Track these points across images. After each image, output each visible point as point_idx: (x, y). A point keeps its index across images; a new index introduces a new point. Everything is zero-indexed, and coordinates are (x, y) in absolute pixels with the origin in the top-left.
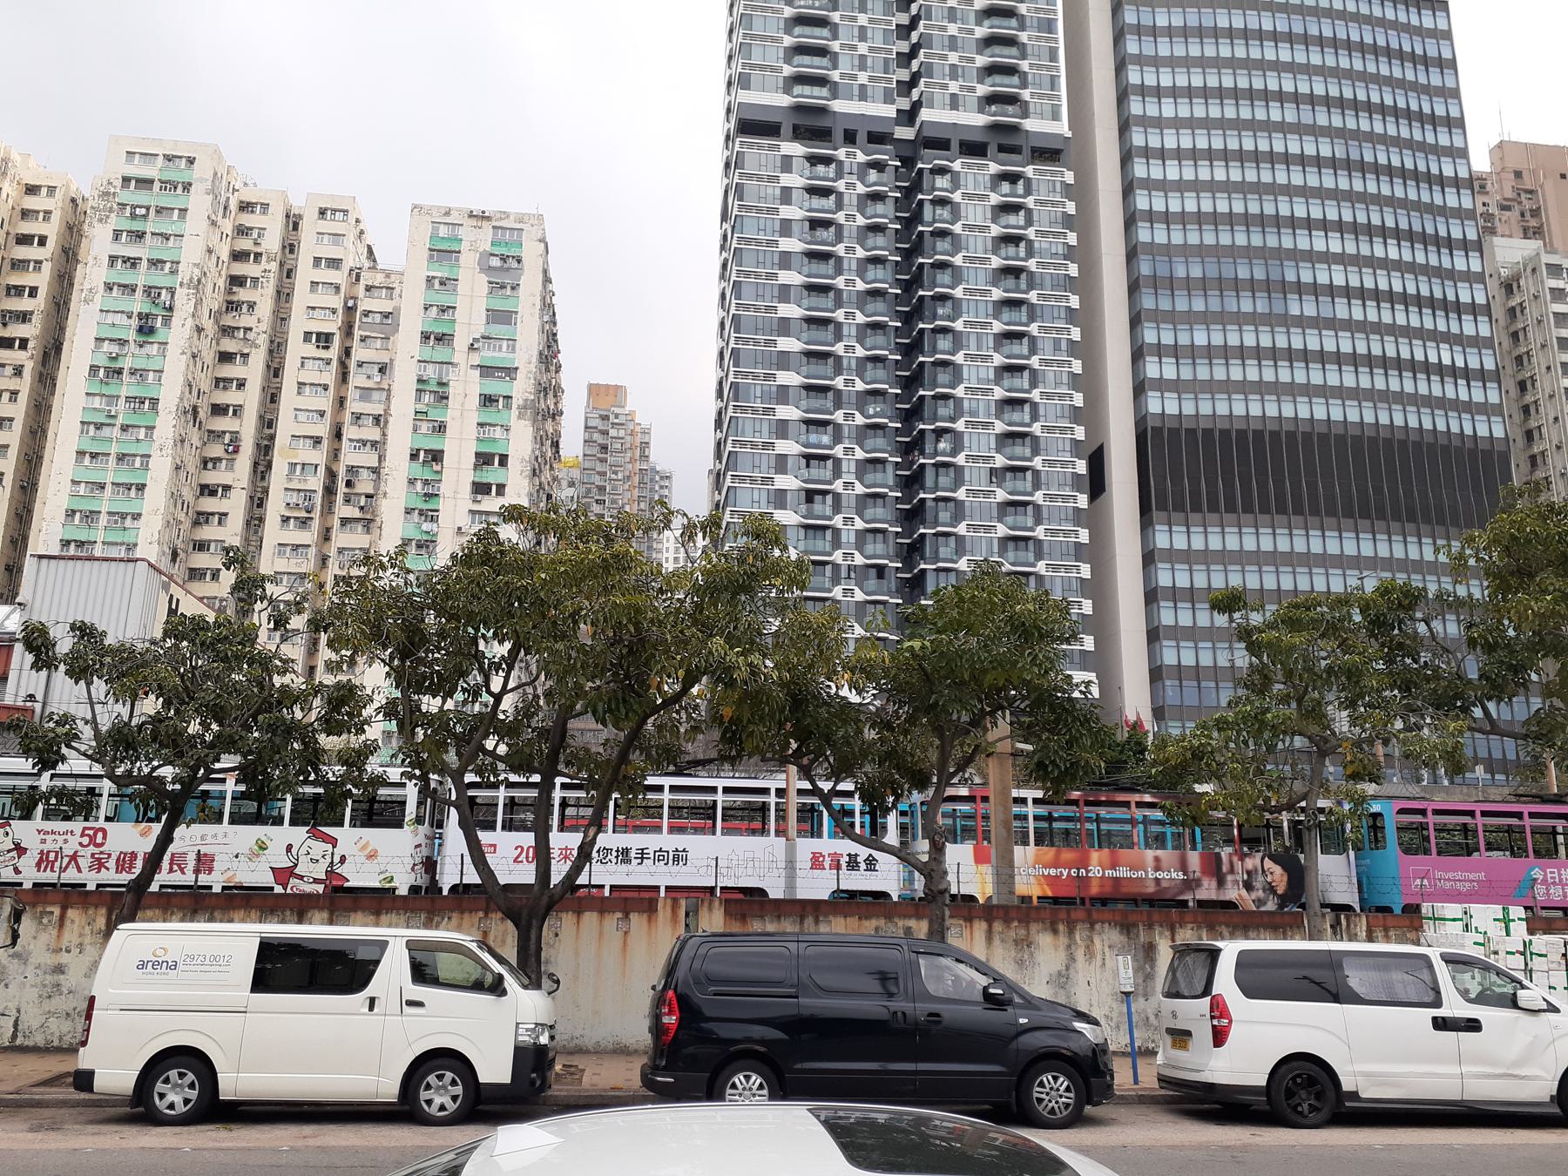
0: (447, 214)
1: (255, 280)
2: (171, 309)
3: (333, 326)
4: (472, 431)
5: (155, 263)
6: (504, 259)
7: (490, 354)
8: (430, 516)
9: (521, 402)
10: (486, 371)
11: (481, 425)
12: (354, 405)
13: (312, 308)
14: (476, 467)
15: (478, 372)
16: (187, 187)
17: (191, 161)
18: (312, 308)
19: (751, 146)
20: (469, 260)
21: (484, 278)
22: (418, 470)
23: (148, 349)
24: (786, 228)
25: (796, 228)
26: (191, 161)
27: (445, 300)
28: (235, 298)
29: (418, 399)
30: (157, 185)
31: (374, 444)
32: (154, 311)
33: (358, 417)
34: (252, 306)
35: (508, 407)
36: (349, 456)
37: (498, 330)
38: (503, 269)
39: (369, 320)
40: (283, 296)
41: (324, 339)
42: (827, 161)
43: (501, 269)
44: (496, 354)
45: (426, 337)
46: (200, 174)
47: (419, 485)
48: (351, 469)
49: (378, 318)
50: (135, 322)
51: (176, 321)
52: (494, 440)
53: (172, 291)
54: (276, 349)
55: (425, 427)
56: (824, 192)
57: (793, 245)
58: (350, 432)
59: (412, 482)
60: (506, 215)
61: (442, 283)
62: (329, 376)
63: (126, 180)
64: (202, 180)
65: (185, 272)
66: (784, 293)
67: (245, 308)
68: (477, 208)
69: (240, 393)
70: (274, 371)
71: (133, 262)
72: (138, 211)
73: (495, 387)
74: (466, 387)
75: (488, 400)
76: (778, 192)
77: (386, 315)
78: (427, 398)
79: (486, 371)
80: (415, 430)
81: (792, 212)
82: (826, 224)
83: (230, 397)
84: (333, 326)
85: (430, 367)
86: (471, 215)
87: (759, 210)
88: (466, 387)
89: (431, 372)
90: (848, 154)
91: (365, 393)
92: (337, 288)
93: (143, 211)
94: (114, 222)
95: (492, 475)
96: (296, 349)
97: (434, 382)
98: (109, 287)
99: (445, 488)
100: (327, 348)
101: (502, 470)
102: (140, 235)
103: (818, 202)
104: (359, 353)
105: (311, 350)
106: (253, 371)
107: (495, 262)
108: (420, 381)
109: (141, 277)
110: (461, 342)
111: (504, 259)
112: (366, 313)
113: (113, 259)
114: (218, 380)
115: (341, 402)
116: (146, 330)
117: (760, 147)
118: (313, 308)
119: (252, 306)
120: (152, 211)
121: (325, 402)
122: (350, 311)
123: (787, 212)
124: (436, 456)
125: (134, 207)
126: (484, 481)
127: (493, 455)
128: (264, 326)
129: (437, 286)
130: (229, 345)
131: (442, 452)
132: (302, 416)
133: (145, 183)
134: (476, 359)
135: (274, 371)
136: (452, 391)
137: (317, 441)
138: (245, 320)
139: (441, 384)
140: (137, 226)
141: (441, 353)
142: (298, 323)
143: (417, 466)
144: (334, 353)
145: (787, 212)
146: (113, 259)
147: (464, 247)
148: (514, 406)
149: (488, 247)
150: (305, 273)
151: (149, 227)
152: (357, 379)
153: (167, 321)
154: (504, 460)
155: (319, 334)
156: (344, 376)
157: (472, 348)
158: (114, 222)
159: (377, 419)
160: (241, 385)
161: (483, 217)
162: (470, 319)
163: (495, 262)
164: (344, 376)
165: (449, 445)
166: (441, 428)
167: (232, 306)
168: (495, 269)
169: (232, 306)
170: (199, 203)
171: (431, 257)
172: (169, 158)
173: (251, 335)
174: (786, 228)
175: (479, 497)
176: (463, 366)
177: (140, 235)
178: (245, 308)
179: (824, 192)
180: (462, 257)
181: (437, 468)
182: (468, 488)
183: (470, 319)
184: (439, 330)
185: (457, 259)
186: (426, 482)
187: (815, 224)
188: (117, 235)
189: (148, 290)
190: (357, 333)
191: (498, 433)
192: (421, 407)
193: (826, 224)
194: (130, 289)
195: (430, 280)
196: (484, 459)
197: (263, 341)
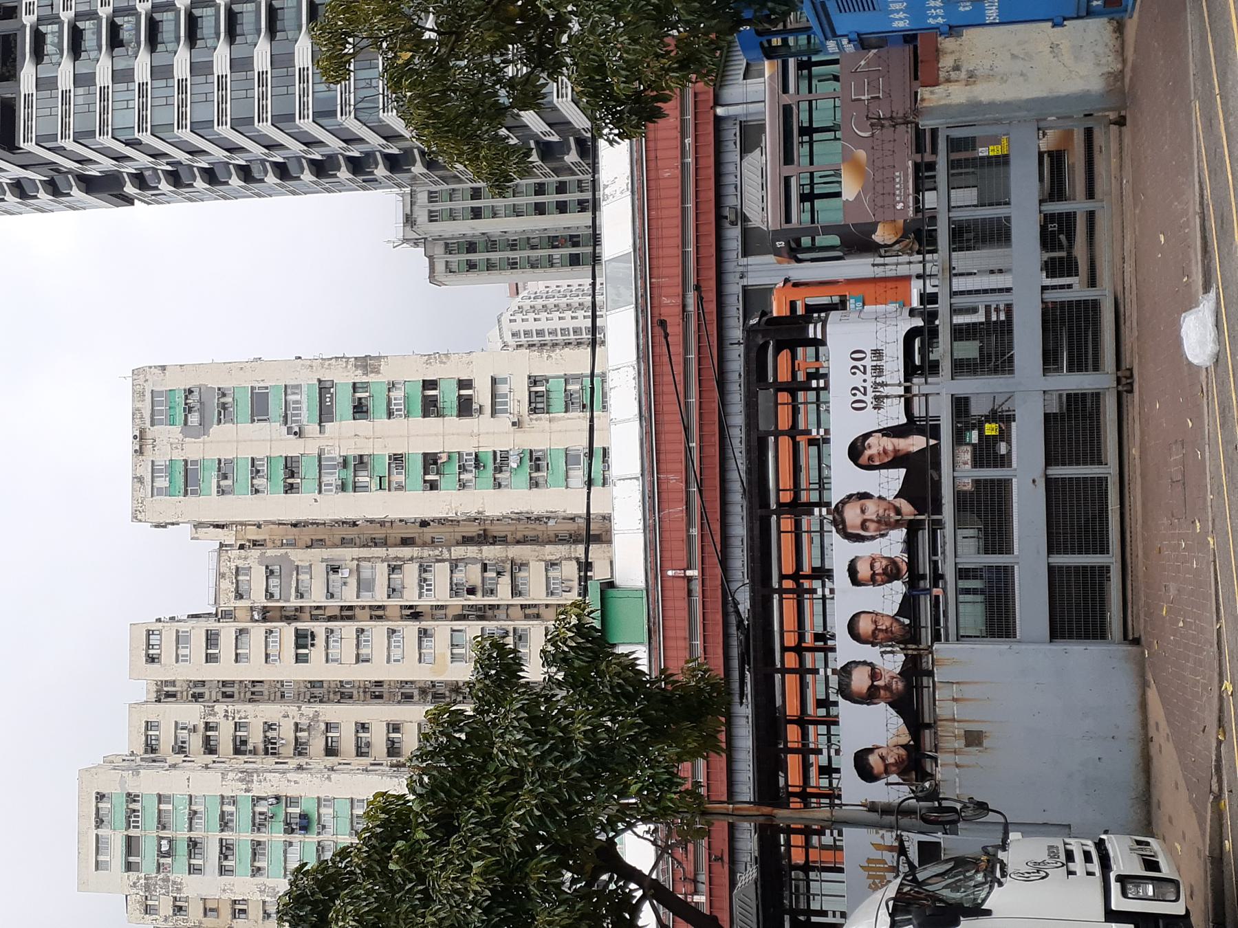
0: (140, 480)
1: (237, 726)
2: (277, 798)
3: (288, 632)
4: (398, 423)
5: (225, 824)
6: (189, 409)
7: (304, 413)
8: (501, 461)
9: (359, 372)
10: (325, 414)
11: (390, 414)
12: (379, 596)
13: (267, 657)
14: (439, 415)
15: (328, 425)
16: (132, 798)
17: (100, 797)
18: (267, 657)
19: (27, 129)
20: (194, 450)
21: (215, 428)
22: (449, 479)
23: (327, 819)
24: (122, 76)
25: (121, 64)
26: (100, 797)
27: (244, 472)
28: (261, 746)
29: (365, 488)
30: (133, 832)
31: (423, 569)
32: (282, 817)
33: (392, 591)
34: (269, 727)
35: (366, 386)
36: (440, 594)
37: (275, 408)
38: (200, 406)
39: (276, 592)
40: (254, 692)
41: (303, 639)
42: (39, 39)
43: (202, 412)
44: (304, 406)
45: (290, 489)
46: (113, 784)
47: (464, 476)
48: (455, 590)
49: (274, 581)
50: (297, 838)
51: (292, 792)
52: (407, 398)
53: (257, 800)
54: (316, 692)
55: (398, 478)
56: (77, 36)
57: (142, 65)
58: (411, 597)
59: (463, 485)
60: (136, 412)
61: (225, 477)
62: (347, 629)
63: (129, 867)
64: (123, 781)
65: (233, 787)
66: (200, 69)
67: (270, 734)
68: (127, 445)
69: (373, 728)
70: (343, 693)
71: (226, 850)
72: (165, 848)
73: (344, 403)
74: (346, 437)
75: (360, 410)
76: (80, 91)
77: (270, 573)
78: (363, 478)
79: (325, 414)
80: (400, 487)
81: (103, 70)
82: (114, 29)
83: (378, 738)
84: (288, 632)
85: (325, 479)
86: (140, 452)
87: (104, 111)
88: (346, 437)
89: (331, 479)
90: (29, 12)
91: (364, 585)
92: (241, 632)
93: (164, 842)
94: (179, 874)
95: (448, 396)
96: (317, 669)
97: (343, 474)
98: (257, 871)
99: (468, 447)
100: (313, 636)
101: (442, 384)
102: (193, 845)
103: (89, 41)
104: (317, 597)
105: (316, 653)
106: (345, 715)
107: (194, 419)
108: (343, 487)
109: (242, 836)
110: (293, 447)
111: (189, 409)
112: (269, 595)
113: (222, 871)
114: (360, 753)
115: (378, 613)
116: (305, 824)
117: (29, 118)
118: (267, 656)
119: (269, 727)
120: (163, 833)
121: (378, 631)
122: (266, 615)
123: (103, 76)
124: (430, 461)
125: (161, 854)
126: (455, 404)
127: (425, 397)
128: (292, 710)
129: (229, 482)
130: (317, 745)
131: (425, 455)
132: (396, 654)
133: (131, 845)
134: (312, 428)
135: (343, 693)
136: (352, 451)
137: (423, 633)
138: (286, 733)
139: (345, 464)
140: (182, 849)
141: (308, 470)
142: (287, 670)
143: (443, 482)
144: (319, 628)
145: (103, 76)
146: (222, 871)
147: (178, 456)
148: (365, 379)
149: (176, 430)
150: (225, 670)
151: (182, 834)
152: (349, 596)
153: (291, 801)
154: (429, 384)
155: (298, 646)
156: (347, 613)
157: (299, 434)
158: (179, 874)
159: (393, 569)
160: (363, 727)
161: (141, 437)
162: (266, 440)
163: (194, 419)
164: (347, 613)
165: (416, 449)
166: (397, 459)
167: (270, 748)
168: (202, 418)
169: (270, 748)
170: (150, 782)
171: (194, 493)
172: (99, 822)
173: (304, 722)
174: (122, 76)
175: (475, 406)
176: (322, 443)
177: (193, 845)
178: (270, 734)
179: (77, 36)
180: (192, 457)
181: (444, 458)
182: (466, 421)
183: (266, 440)
184: (281, 473)
185: (195, 462)
186: (463, 469)
187: (115, 41)
188: (193, 870)
189: (257, 826)
190: (294, 602)
191: (397, 394)
192: (375, 484)
193: (114, 29)
194: (257, 846)
195: (222, 491)
196: (430, 407)
197: (308, 710)
